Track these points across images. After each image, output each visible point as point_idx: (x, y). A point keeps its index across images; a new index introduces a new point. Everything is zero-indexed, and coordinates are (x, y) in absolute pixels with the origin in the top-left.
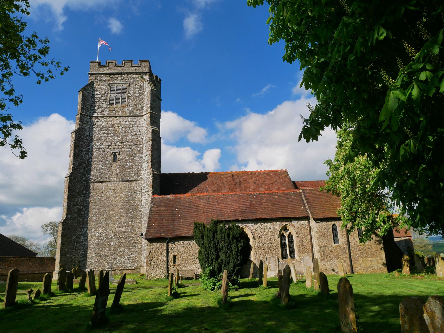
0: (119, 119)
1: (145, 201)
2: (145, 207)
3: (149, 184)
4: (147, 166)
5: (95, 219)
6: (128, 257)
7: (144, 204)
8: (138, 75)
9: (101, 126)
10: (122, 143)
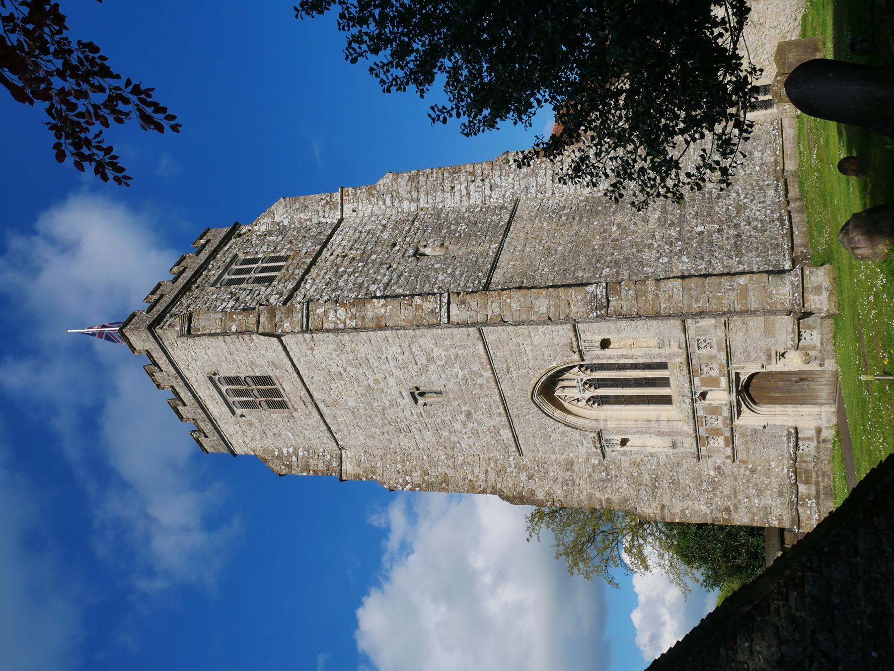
0: (323, 258)
4: (483, 180)
5: (611, 270)
6: (745, 198)
8: (230, 242)
9: (324, 287)
10: (394, 245)
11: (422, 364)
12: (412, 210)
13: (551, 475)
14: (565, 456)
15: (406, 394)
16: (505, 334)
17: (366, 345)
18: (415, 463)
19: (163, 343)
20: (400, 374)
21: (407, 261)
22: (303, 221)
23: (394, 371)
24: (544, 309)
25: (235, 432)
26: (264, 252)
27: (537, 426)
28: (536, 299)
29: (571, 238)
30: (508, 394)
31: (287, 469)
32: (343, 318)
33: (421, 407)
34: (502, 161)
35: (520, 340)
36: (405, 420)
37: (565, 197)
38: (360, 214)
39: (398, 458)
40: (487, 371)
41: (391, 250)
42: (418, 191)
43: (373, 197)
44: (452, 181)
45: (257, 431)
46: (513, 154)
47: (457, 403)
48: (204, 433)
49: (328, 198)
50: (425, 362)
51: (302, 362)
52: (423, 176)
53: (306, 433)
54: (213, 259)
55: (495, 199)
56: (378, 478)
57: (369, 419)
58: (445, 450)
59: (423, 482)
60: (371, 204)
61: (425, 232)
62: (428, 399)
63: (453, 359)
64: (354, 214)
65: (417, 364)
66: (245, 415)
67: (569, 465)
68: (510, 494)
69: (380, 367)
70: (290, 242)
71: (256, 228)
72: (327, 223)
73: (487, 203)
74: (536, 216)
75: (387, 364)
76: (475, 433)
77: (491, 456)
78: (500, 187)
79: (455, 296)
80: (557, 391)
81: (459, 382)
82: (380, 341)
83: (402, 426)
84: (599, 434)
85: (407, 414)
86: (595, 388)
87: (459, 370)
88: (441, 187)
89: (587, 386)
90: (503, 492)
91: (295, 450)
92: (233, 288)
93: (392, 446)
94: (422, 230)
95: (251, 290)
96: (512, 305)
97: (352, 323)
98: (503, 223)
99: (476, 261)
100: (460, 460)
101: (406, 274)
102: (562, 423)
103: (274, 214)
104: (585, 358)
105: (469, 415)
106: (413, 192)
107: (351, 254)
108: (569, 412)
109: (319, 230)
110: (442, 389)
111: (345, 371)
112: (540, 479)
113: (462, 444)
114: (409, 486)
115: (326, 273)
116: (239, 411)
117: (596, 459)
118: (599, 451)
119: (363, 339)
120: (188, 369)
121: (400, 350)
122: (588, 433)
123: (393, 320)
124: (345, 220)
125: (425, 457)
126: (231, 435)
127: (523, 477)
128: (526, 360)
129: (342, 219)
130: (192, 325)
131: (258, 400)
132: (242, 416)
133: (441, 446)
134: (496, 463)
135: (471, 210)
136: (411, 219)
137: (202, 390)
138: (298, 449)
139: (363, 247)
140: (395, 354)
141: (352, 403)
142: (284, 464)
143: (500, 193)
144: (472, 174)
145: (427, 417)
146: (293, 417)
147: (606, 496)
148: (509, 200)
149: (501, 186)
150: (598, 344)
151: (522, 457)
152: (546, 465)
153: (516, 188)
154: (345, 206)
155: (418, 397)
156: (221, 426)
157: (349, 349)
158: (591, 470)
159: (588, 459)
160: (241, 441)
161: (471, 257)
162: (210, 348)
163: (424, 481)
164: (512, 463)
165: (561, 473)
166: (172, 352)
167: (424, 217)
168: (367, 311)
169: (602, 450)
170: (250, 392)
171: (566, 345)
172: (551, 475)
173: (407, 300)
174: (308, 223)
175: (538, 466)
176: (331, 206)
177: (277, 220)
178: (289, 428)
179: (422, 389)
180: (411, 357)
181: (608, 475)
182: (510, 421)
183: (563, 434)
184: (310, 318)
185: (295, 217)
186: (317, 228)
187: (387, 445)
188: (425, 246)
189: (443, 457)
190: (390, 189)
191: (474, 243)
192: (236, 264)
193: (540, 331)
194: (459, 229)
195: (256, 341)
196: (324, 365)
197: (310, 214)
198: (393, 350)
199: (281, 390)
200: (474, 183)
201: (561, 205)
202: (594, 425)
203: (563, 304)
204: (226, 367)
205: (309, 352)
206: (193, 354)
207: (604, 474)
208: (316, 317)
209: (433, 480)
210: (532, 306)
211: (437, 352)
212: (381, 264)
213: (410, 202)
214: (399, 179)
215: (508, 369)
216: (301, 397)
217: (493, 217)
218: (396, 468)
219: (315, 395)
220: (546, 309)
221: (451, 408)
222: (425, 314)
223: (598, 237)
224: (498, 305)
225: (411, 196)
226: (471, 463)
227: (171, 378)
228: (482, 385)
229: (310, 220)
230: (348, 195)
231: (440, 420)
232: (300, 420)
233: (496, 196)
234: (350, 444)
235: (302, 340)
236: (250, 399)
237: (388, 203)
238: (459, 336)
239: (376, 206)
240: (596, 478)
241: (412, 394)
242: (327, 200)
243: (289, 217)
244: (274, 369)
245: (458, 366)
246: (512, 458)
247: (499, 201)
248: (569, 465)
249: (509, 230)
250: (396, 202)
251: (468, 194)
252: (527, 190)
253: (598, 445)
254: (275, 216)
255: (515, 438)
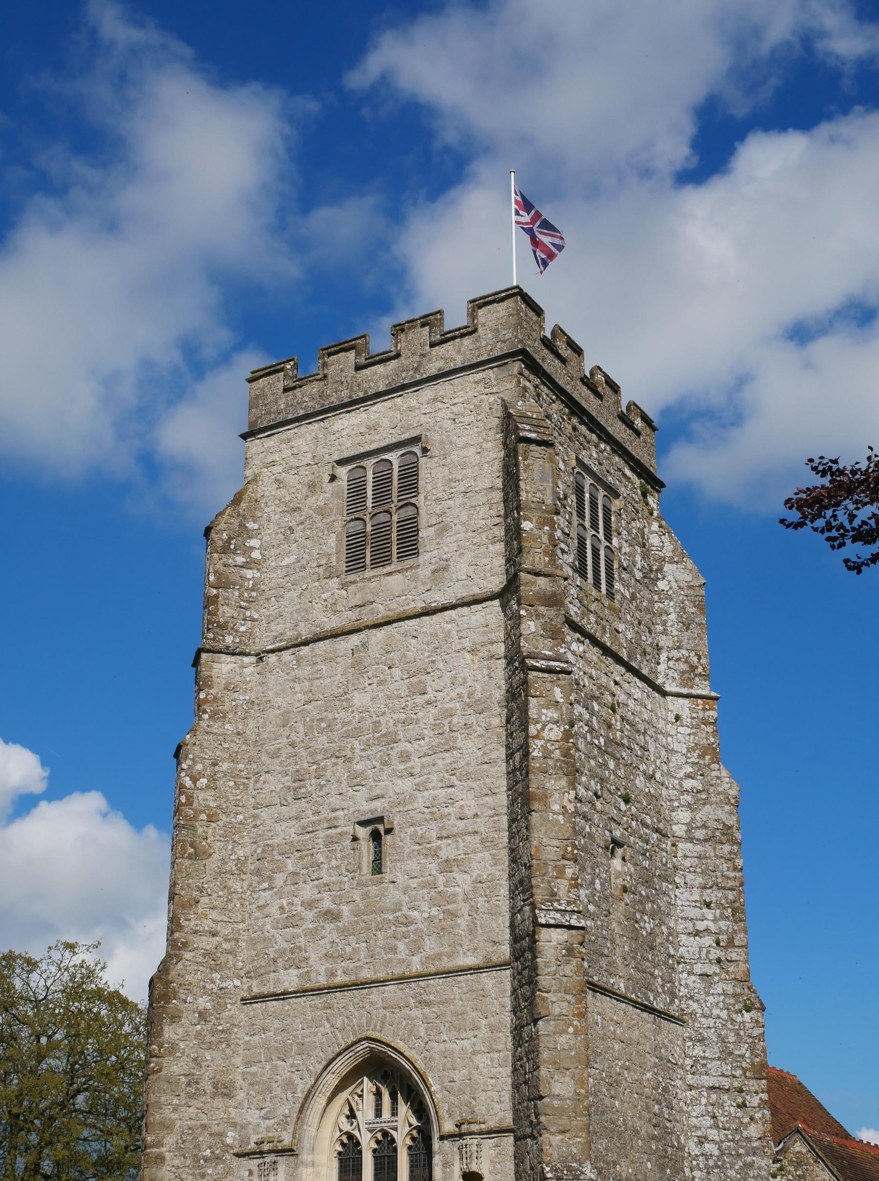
1: (713, 1134)
2: (718, 1167)
3: (742, 1056)
4: (719, 961)
7: (709, 1147)
10: (627, 800)
11: (439, 848)
12: (675, 828)
13: (206, 1054)
14: (240, 1082)
15: (378, 807)
16: (496, 1007)
17: (480, 753)
18: (232, 798)
19: (492, 368)
20: (419, 804)
21: (605, 827)
22: (664, 618)
23: (426, 794)
24: (557, 1089)
25: (295, 451)
26: (620, 548)
27: (307, 1040)
28: (573, 1077)
29: (630, 1123)
30: (375, 995)
31: (220, 543)
32: (545, 734)
33: (350, 829)
34: (748, 999)
35: (484, 1032)
36: (322, 793)
37: (685, 1108)
38: (671, 729)
39: (241, 766)
40: (422, 964)
41: (619, 796)
42: (706, 840)
43: (699, 756)
44: (720, 905)
45: (299, 496)
46: (760, 1020)
47: (357, 898)
48: (294, 388)
49: (700, 670)
50: (443, 854)
51: (448, 626)
52: (730, 853)
53: (293, 594)
54: (612, 449)
55: (687, 981)
56: (203, 724)
57: (324, 725)
58: (255, 857)
59: (195, 811)
60: (688, 751)
61: (642, 854)
62: (366, 848)
63: (449, 907)
64: (671, 718)
65: (439, 838)
66: (334, 484)
67: (223, 1090)
68: (173, 974)
69: (434, 769)
70: (633, 597)
71: (655, 526)
72: (659, 664)
73: (681, 966)
74: (661, 1058)
75: (440, 785)
76: (291, 921)
77: (242, 944)
78: (706, 993)
79: (580, 938)
80: (370, 1084)
81: (400, 910)
82: (488, 781)
83: (310, 785)
84: (289, 1151)
85: (335, 801)
86: (375, 1151)
87: (426, 915)
88: (710, 884)
89: (379, 1136)
90: (177, 963)
91: (255, 562)
92: (572, 499)
93: (264, 757)
94: (647, 850)
95: (568, 535)
96: (564, 1036)
97: (536, 751)
98: (652, 998)
99: (603, 955)
100: (236, 885)
101: (588, 829)
102: (313, 1086)
103: (677, 563)
104: (446, 1142)
105: (333, 916)
106: (704, 831)
107: (616, 721)
108: (330, 1100)
109: (649, 649)
110: (388, 877)
111: (429, 703)
112: (199, 1033)
113: (268, 893)
114: (188, 782)
115: (591, 677)
116: (343, 472)
117: (235, 1139)
118: (252, 1146)
119: (491, 751)
120: (435, 400)
121: (469, 813)
122: (291, 1131)
123: (541, 825)
124: (662, 699)
125: (241, 817)
126: (289, 440)
127: (204, 1003)
128: (445, 1037)
129: (664, 694)
130: (533, 447)
131: (367, 518)
132: (333, 478)
133: (263, 851)
134: (229, 952)
135: (671, 938)
136: (661, 826)
137: (391, 413)
138: (258, 570)
139: (625, 741)
140: (462, 803)
141: (359, 699)
142: (230, 539)
143: (696, 991)
144: (731, 943)
145: (328, 836)
146: (329, 577)
147: (168, 1156)
148: (683, 1006)
149: (707, 994)
150: (474, 1168)
151: (239, 1002)
152: (224, 1046)
153: (703, 1020)
154: (686, 702)
155: (369, 829)
156: (311, 427)
157: (472, 719)
158: (216, 1129)
159: (234, 1125)
160: (276, 457)
161: (609, 945)
162: (478, 457)
163: (197, 813)
164: (228, 984)
165: (210, 1073)
166: (471, 378)
167: (662, 850)
168: (555, 779)
169: (255, 1153)
170: (386, 507)
171: (473, 1112)
172: (206, 1054)
173: (573, 851)
174: (659, 628)
175: (222, 1031)
176: (687, 675)
177: (667, 568)
178: (304, 562)
179: (387, 839)
180: (455, 830)
181: (205, 1161)
182: (318, 991)
183: (289, 1085)
184: (546, 675)
185: (672, 604)
186: (651, 645)
187: (267, 747)
188: (624, 859)
189: (241, 853)
190: (711, 790)
191: (627, 948)
192: (605, 496)
193: (501, 1069)
194: (646, 918)
195: (491, 548)
196: (441, 665)
197: (675, 633)
198: (469, 803)
199: (388, 569)
200: (714, 945)
201: (674, 1102)
202: (306, 1144)
203: (564, 1122)
204: (440, 476)
205: (467, 643)
206: (467, 420)
207: (208, 1153)
208: (548, 685)
209: (200, 830)
210: (562, 1070)
211: (463, 881)
212: (602, 780)
213: (687, 824)
214: (727, 808)
215: (428, 1004)
216: (372, 603)
217: (659, 980)
218: (223, 760)
219: (379, 635)
220: (556, 1093)
221: (347, 886)
222: (549, 882)
223: (630, 1171)
224: (564, 1012)
225: (698, 828)
226: (230, 906)
227: (417, 358)
228: (394, 950)
229: (665, 632)
230: (704, 709)
231: (322, 860)
232: (323, 590)
233: (691, 984)
234: (268, 675)
235: (492, 636)
236: (369, 503)
237: (688, 784)
238: (495, 925)
239: (683, 760)
240: (201, 1139)
241: (380, 820)
242: (697, 667)
243: (670, 592)
244: (432, 567)
245: (434, 911)
246: (237, 983)
247: (682, 989)
248: (223, 1090)
249: (642, 1010)
250: (688, 798)
251: (697, 933)
252: (699, 1041)
253: (266, 1147)
254: (675, 566)
255: (282, 996)
